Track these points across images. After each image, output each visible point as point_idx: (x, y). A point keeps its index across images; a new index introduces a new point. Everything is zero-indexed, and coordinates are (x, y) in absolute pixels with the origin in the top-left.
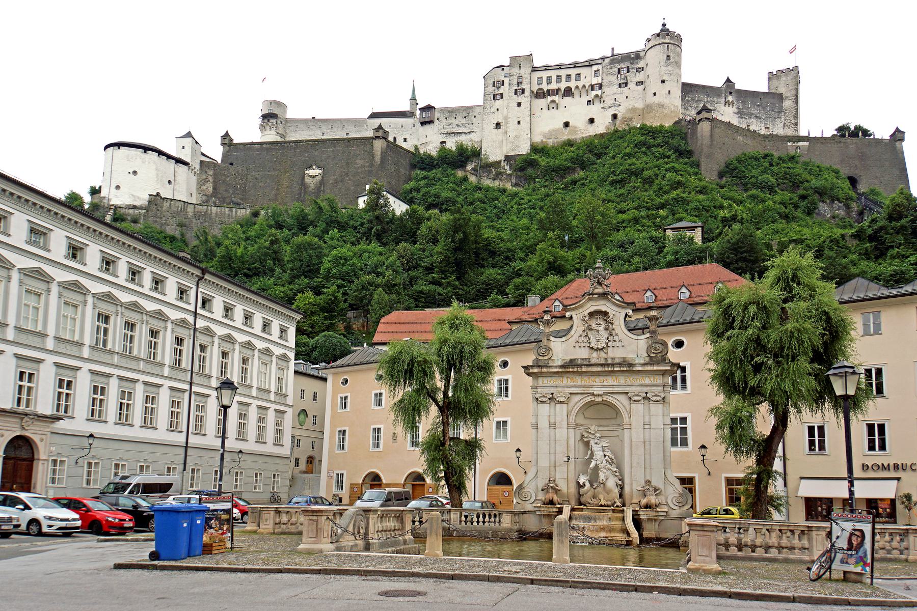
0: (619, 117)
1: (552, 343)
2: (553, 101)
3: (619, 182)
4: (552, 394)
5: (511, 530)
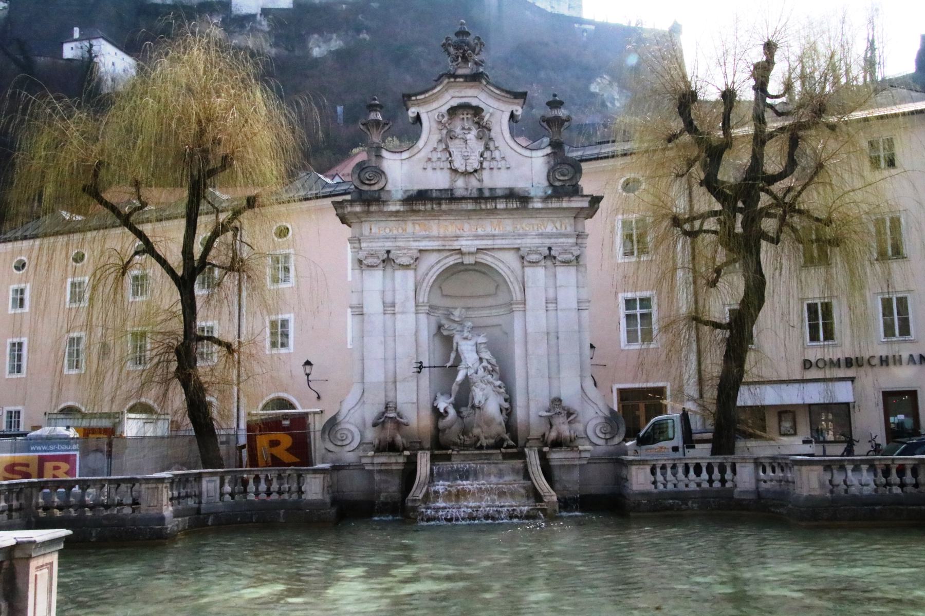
4: (388, 252)
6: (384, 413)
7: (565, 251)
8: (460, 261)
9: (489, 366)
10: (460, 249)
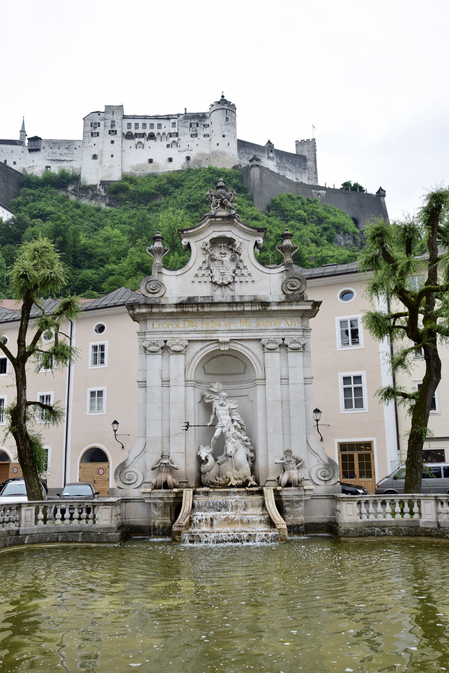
0: (192, 158)
1: (164, 276)
2: (140, 142)
3: (193, 206)
4: (165, 341)
5: (110, 529)
6: (160, 460)
7: (295, 342)
8: (218, 348)
9: (239, 425)
10: (218, 340)
